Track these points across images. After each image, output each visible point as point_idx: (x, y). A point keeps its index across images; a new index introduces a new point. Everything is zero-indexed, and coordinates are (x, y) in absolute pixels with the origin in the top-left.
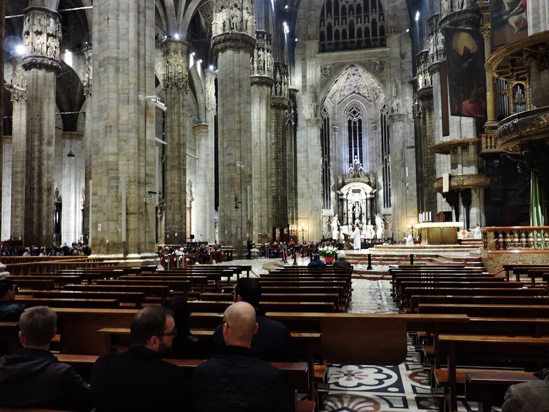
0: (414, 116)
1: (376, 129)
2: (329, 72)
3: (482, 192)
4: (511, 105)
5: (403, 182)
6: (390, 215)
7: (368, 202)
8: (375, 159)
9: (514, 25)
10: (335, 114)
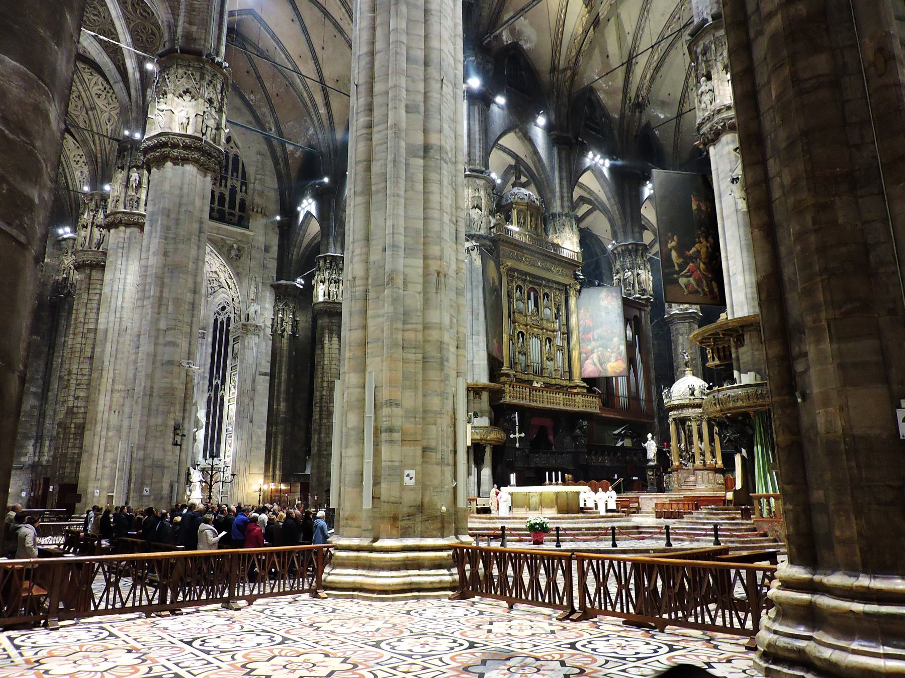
0: (274, 333)
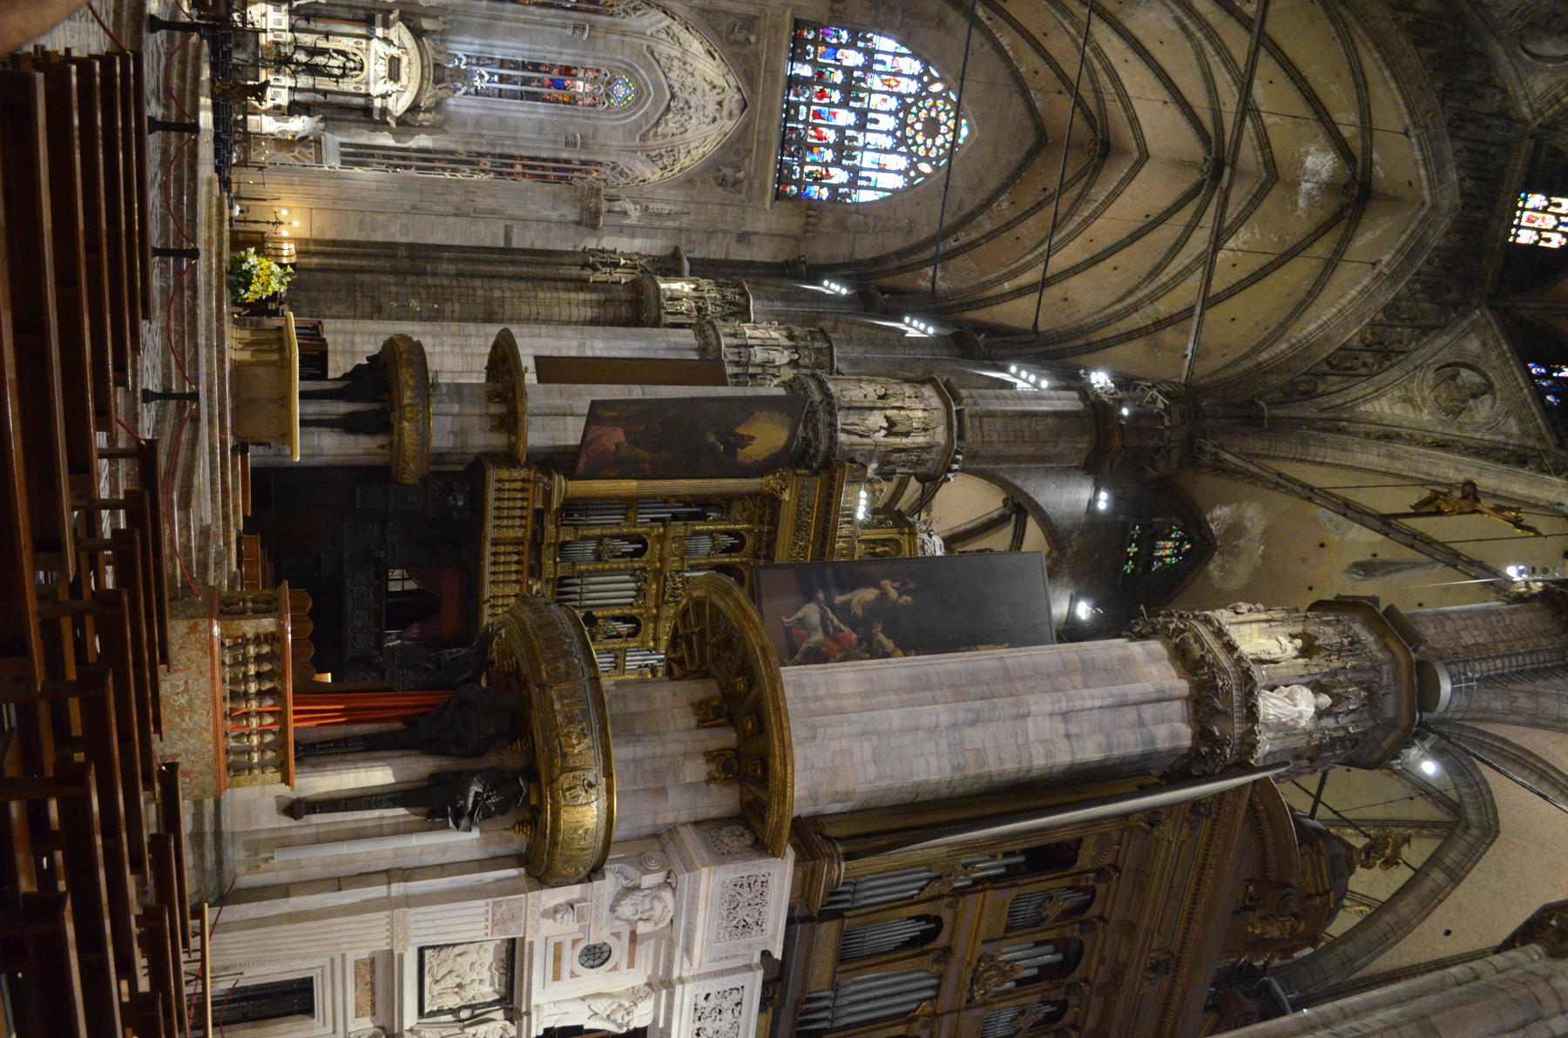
0: (591, 252)
1: (567, 144)
2: (741, 38)
3: (379, 460)
4: (598, 531)
5: (414, 207)
6: (319, 160)
7: (361, 101)
8: (485, 132)
9: (800, 614)
10: (624, 34)
